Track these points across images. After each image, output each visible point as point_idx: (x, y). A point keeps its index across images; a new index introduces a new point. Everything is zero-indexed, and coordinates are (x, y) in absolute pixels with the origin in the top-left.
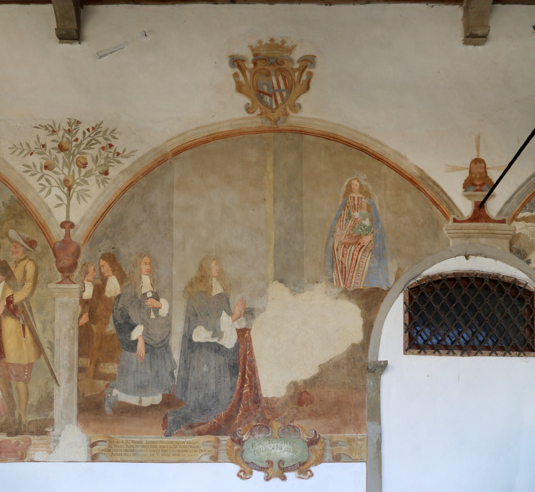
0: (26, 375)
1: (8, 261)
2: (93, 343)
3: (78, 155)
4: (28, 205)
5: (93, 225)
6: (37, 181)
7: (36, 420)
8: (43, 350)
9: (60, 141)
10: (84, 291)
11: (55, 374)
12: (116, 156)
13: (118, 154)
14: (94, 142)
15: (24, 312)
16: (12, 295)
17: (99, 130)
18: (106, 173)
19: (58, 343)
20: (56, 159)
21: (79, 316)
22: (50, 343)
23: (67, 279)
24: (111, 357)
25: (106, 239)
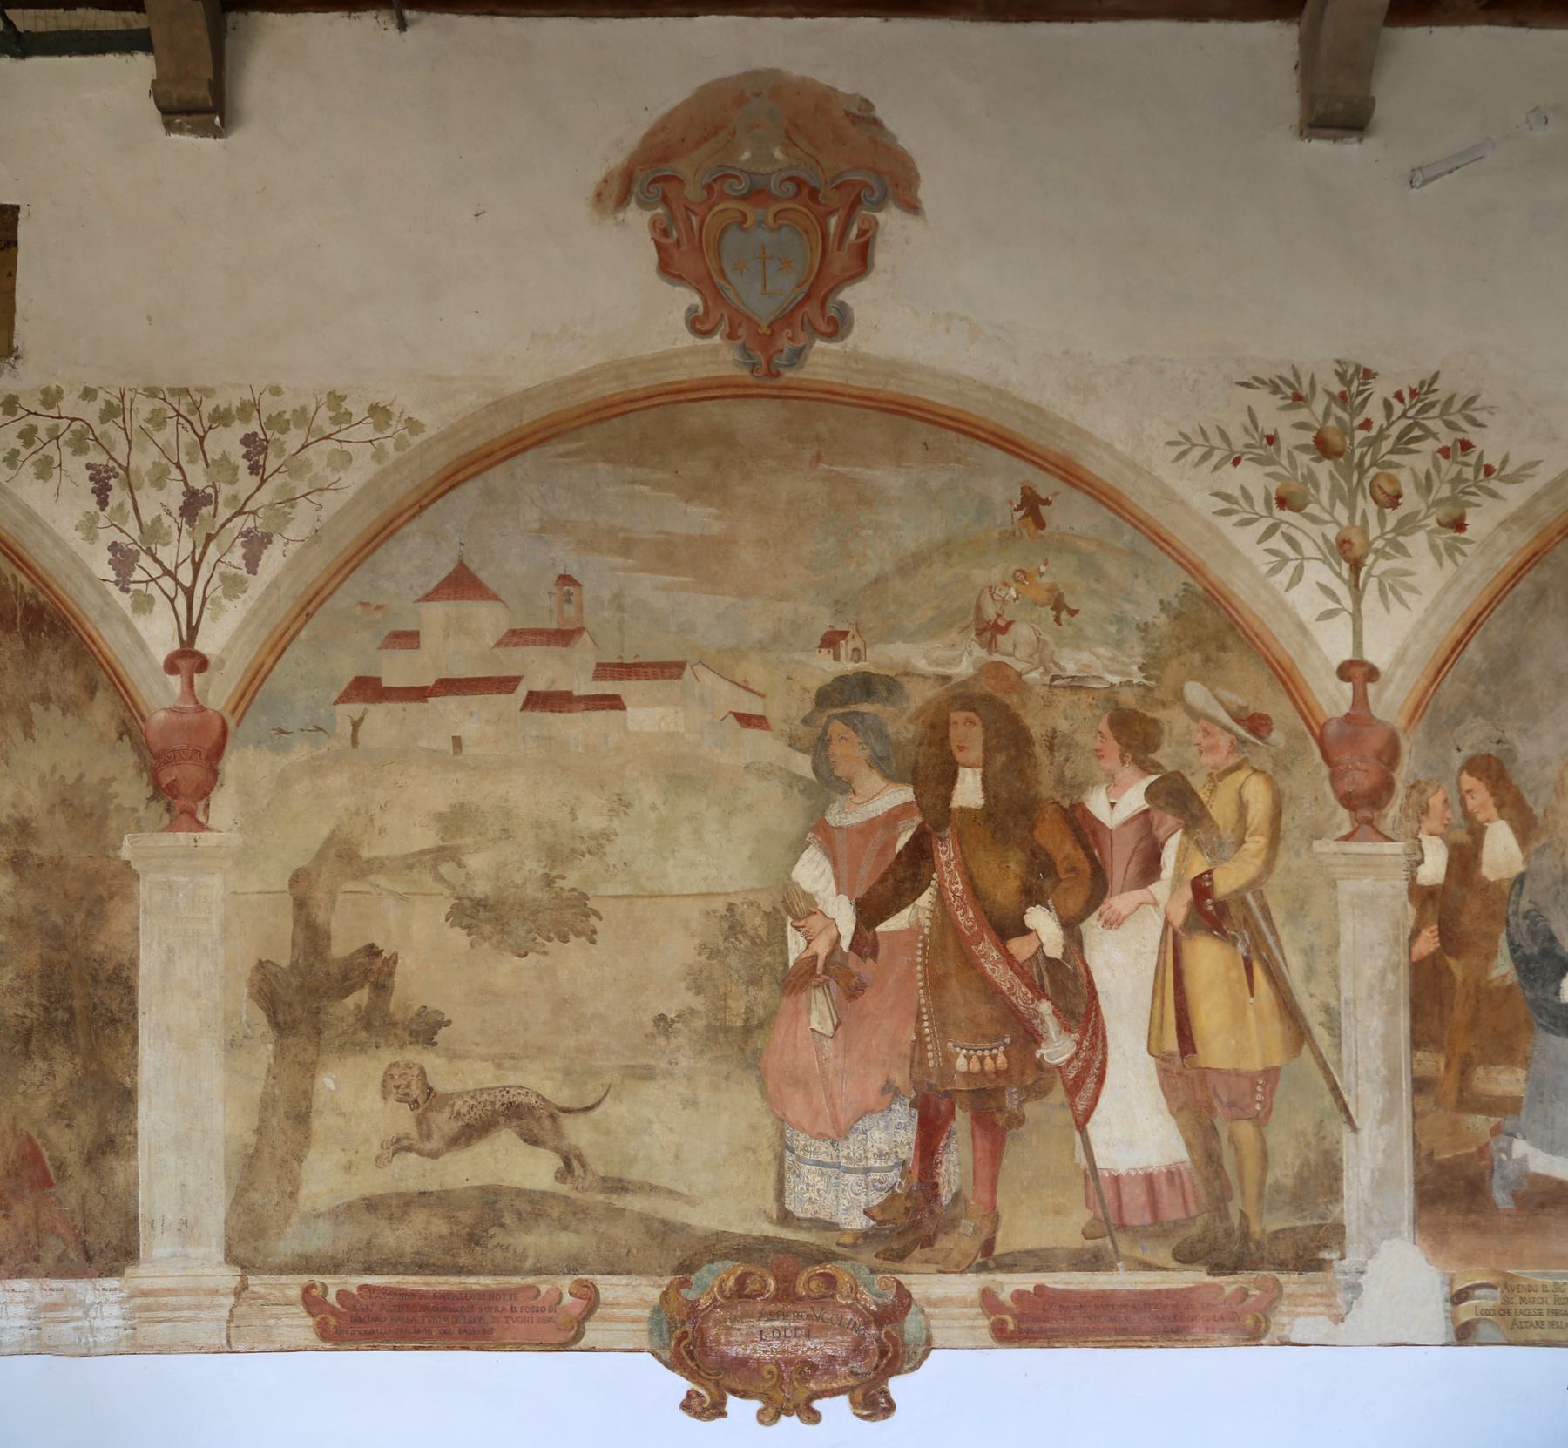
0: (1260, 1102)
1: (1186, 774)
2: (1452, 1009)
3: (1374, 471)
4: (1238, 612)
5: (1431, 673)
6: (1259, 542)
7: (1293, 1229)
8: (1309, 1031)
9: (1318, 426)
10: (1421, 862)
11: (1346, 1098)
12: (1482, 476)
13: (1489, 471)
14: (1417, 432)
15: (1248, 921)
16: (1210, 872)
17: (1431, 398)
18: (1459, 525)
19: (1352, 1010)
20: (1311, 478)
21: (1409, 932)
22: (1327, 1009)
23: (1365, 827)
24: (1506, 1049)
25: (1476, 716)
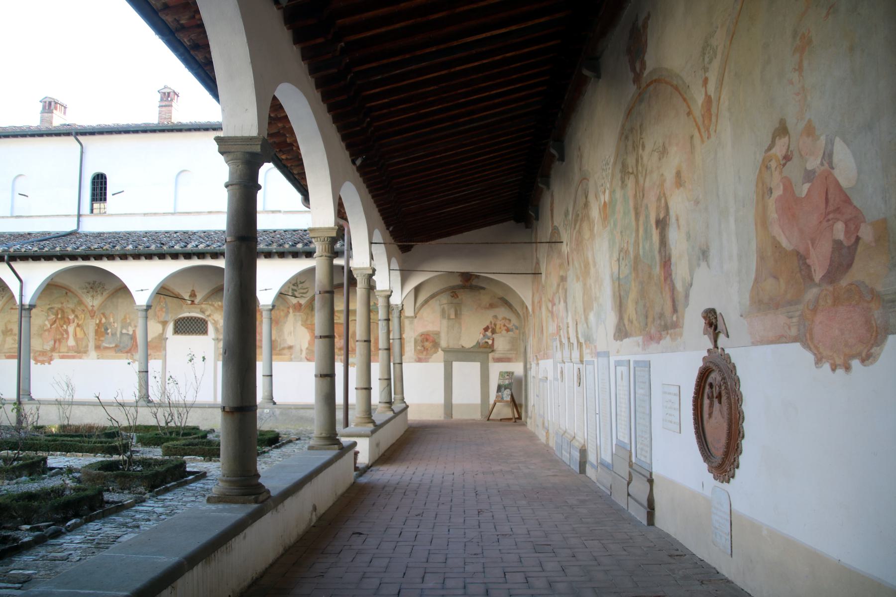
24: (103, 336)
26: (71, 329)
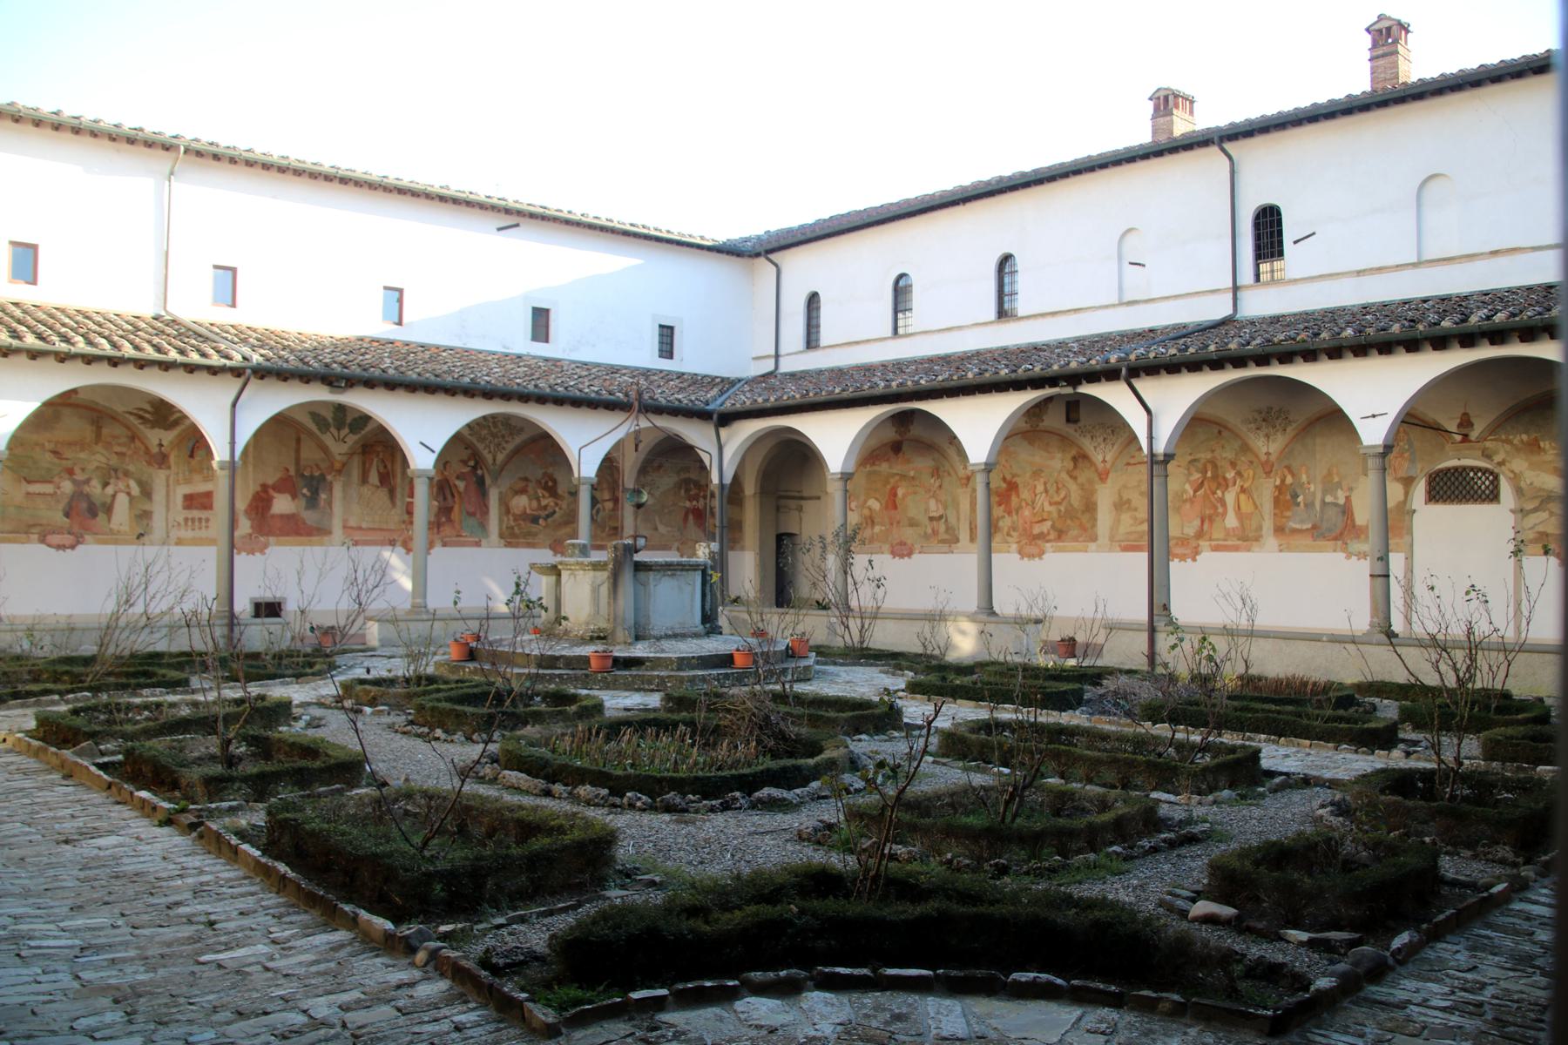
24: (1288, 509)
26: (1230, 497)
